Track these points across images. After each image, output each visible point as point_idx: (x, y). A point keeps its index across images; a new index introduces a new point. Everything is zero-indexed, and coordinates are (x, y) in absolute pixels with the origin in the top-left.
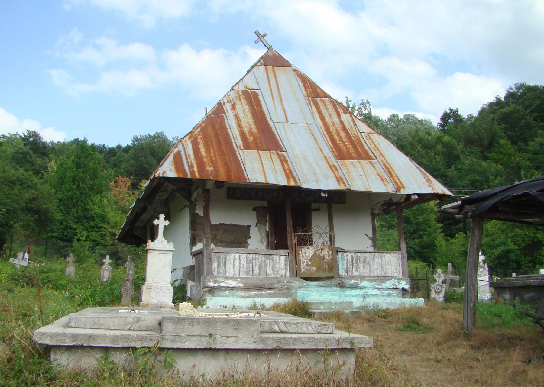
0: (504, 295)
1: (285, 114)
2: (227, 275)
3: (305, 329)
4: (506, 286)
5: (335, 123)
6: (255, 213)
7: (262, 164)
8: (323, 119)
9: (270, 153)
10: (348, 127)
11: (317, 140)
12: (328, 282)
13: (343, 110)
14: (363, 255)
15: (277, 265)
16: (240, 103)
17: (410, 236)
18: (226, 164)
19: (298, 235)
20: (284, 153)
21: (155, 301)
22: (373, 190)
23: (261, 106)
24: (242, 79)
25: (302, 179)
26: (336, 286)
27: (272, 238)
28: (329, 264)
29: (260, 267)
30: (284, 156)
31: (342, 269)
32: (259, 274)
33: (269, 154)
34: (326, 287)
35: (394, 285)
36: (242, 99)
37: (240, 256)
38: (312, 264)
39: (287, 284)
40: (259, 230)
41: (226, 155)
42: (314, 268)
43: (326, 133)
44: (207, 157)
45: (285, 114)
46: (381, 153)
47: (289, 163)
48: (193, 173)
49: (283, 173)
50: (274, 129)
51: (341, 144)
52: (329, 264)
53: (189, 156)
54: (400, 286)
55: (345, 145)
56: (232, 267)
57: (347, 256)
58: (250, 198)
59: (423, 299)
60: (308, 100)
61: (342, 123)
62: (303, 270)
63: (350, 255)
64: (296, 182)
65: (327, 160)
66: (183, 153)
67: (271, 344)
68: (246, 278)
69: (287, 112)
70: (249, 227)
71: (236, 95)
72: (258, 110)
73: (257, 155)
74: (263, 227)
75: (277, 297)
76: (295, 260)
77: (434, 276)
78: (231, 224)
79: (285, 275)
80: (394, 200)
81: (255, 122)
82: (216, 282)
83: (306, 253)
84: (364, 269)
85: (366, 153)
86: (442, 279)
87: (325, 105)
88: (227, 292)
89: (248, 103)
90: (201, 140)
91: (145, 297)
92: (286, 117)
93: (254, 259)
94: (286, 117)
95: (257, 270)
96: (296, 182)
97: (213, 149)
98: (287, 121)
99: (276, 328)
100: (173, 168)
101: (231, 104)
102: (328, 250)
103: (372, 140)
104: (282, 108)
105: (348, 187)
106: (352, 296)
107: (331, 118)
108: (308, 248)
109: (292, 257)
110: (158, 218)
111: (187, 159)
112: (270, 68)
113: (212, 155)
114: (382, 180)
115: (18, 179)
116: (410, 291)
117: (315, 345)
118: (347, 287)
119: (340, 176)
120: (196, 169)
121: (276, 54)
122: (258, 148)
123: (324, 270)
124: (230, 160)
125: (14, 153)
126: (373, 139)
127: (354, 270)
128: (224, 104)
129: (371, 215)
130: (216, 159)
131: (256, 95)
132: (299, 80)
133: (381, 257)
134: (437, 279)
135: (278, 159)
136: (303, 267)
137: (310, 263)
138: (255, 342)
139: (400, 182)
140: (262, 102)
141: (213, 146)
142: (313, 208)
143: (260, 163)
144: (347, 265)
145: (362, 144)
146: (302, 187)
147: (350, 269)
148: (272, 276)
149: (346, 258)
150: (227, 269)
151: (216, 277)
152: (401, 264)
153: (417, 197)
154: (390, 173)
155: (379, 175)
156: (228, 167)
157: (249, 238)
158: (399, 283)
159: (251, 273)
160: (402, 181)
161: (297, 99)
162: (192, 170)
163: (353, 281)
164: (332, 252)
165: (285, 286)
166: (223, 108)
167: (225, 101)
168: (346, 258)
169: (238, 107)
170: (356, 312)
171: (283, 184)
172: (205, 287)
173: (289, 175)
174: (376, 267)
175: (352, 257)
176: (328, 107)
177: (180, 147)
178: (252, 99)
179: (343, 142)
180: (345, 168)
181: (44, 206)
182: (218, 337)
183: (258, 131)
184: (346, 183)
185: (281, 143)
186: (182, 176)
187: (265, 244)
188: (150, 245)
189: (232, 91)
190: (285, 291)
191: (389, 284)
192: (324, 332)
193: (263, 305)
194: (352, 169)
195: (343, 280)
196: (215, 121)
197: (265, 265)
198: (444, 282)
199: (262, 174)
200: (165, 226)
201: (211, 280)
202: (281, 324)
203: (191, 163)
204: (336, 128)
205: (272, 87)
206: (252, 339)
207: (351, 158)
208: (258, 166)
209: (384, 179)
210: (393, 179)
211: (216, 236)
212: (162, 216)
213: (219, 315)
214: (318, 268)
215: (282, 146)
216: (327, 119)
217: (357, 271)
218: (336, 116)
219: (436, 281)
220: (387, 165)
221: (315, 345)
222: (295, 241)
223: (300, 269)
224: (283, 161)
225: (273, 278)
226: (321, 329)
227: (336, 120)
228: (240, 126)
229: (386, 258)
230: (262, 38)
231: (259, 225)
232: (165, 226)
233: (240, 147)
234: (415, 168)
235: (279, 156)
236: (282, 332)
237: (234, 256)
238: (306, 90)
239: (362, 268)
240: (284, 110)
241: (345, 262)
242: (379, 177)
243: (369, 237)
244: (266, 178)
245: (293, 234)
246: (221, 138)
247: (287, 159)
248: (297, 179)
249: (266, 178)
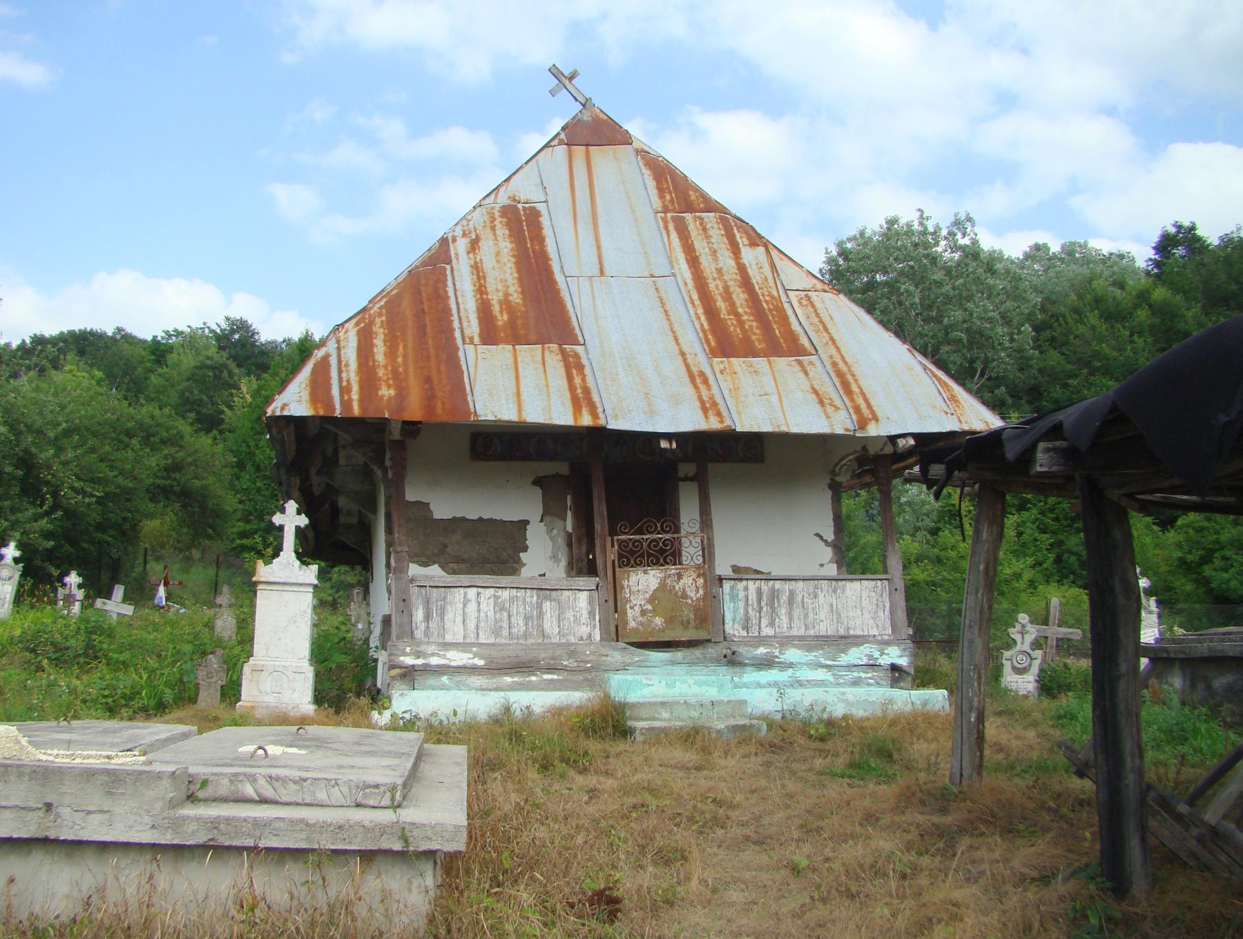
0: (1170, 680)
1: (600, 257)
2: (449, 638)
3: (322, 796)
4: (1173, 655)
5: (725, 269)
6: (537, 493)
7: (517, 378)
8: (693, 262)
9: (543, 349)
10: (756, 279)
11: (670, 313)
12: (698, 652)
13: (749, 238)
14: (787, 586)
15: (569, 615)
16: (491, 235)
17: (1070, 526)
18: (428, 380)
19: (620, 542)
20: (579, 349)
21: (271, 700)
22: (794, 430)
23: (541, 240)
24: (508, 180)
25: (613, 409)
26: (717, 661)
27: (579, 548)
28: (696, 609)
29: (527, 618)
30: (577, 356)
31: (734, 620)
32: (525, 636)
33: (540, 351)
34: (692, 663)
35: (870, 657)
36: (498, 226)
37: (479, 594)
38: (654, 610)
39: (591, 657)
40: (549, 531)
41: (433, 359)
42: (658, 621)
43: (695, 296)
44: (385, 367)
45: (600, 257)
46: (832, 339)
47: (587, 371)
48: (346, 404)
49: (568, 395)
50: (565, 294)
51: (731, 321)
52: (696, 609)
53: (347, 365)
54: (885, 661)
55: (741, 323)
56: (459, 619)
57: (746, 589)
58: (526, 457)
59: (945, 692)
60: (665, 220)
61: (742, 269)
62: (632, 624)
64: (595, 415)
65: (685, 360)
66: (333, 361)
67: (193, 833)
68: (493, 645)
69: (604, 251)
71: (486, 217)
72: (534, 251)
73: (510, 356)
74: (559, 523)
75: (566, 689)
76: (614, 601)
77: (1011, 630)
78: (480, 519)
80: (872, 451)
81: (520, 279)
82: (418, 655)
83: (643, 582)
84: (791, 619)
85: (792, 338)
86: (1029, 638)
87: (705, 229)
88: (445, 679)
89: (510, 236)
90: (382, 326)
91: (249, 692)
92: (601, 263)
93: (512, 599)
94: (601, 263)
95: (519, 625)
96: (595, 415)
97: (405, 347)
98: (602, 273)
99: (249, 790)
100: (306, 395)
101: (468, 240)
102: (694, 576)
103: (813, 306)
104: (594, 243)
105: (728, 422)
106: (759, 685)
107: (716, 260)
108: (645, 572)
109: (607, 593)
110: (283, 511)
111: (340, 372)
112: (579, 151)
113: (400, 360)
114: (821, 403)
115: (141, 426)
116: (912, 671)
117: (308, 839)
118: (746, 665)
119: (712, 398)
120: (355, 396)
121: (602, 115)
122: (516, 337)
123: (685, 625)
124: (439, 370)
125: (196, 367)
126: (818, 305)
127: (764, 622)
128: (454, 240)
129: (831, 487)
130: (406, 370)
131: (533, 215)
132: (647, 173)
133: (835, 591)
134: (1018, 637)
135: (562, 364)
136: (633, 617)
137: (650, 607)
138: (153, 827)
139: (869, 406)
140: (547, 231)
141: (405, 341)
142: (681, 475)
143: (514, 376)
144: (747, 612)
145: (786, 318)
146: (609, 427)
148: (556, 640)
149: (742, 594)
150: (448, 625)
151: (419, 643)
152: (888, 605)
153: (912, 442)
154: (846, 386)
155: (816, 392)
156: (431, 388)
157: (525, 549)
158: (882, 654)
159: (505, 633)
160: (873, 403)
161: (636, 220)
162: (346, 400)
163: (762, 650)
164: (705, 581)
165: (588, 662)
166: (448, 250)
167: (459, 232)
168: (742, 594)
169: (486, 246)
170: (744, 726)
171: (563, 423)
172: (392, 667)
173: (581, 398)
174: (822, 615)
175: (759, 593)
176: (711, 232)
177: (331, 347)
178: (523, 225)
179: (737, 315)
180: (729, 377)
181: (197, 483)
182: (65, 812)
183: (524, 299)
184: (725, 413)
185: (575, 324)
186: (321, 413)
187: (564, 563)
188: (264, 571)
189: (478, 209)
190: (589, 674)
191: (856, 655)
192: (372, 803)
193: (528, 708)
194: (745, 380)
195: (735, 648)
196: (423, 282)
197: (541, 615)
198: (1036, 645)
199: (513, 399)
200: (298, 528)
201: (408, 649)
202: (262, 782)
203: (348, 381)
204: (726, 282)
205: (578, 193)
206: (148, 820)
207: (750, 351)
208: (505, 382)
209: (827, 402)
210: (852, 400)
211: (445, 546)
212: (292, 506)
213: (89, 757)
214: (670, 620)
215: (577, 331)
216: (706, 262)
217: (772, 624)
218: (728, 254)
219: (1015, 641)
220: (842, 366)
221: (308, 839)
222: (612, 555)
224: (573, 366)
225: (559, 645)
226: (365, 796)
227: (727, 262)
228: (481, 290)
229: (848, 593)
230: (566, 82)
231: (548, 518)
232: (298, 528)
233: (472, 339)
234: (919, 369)
235: (564, 354)
236: (264, 801)
237: (465, 594)
238: (661, 197)
239: (784, 620)
240: (599, 247)
241: (741, 604)
242: (814, 396)
243: (826, 541)
244: (520, 411)
245: (609, 539)
246: (427, 319)
247: (584, 361)
248: (600, 410)
249: (520, 411)
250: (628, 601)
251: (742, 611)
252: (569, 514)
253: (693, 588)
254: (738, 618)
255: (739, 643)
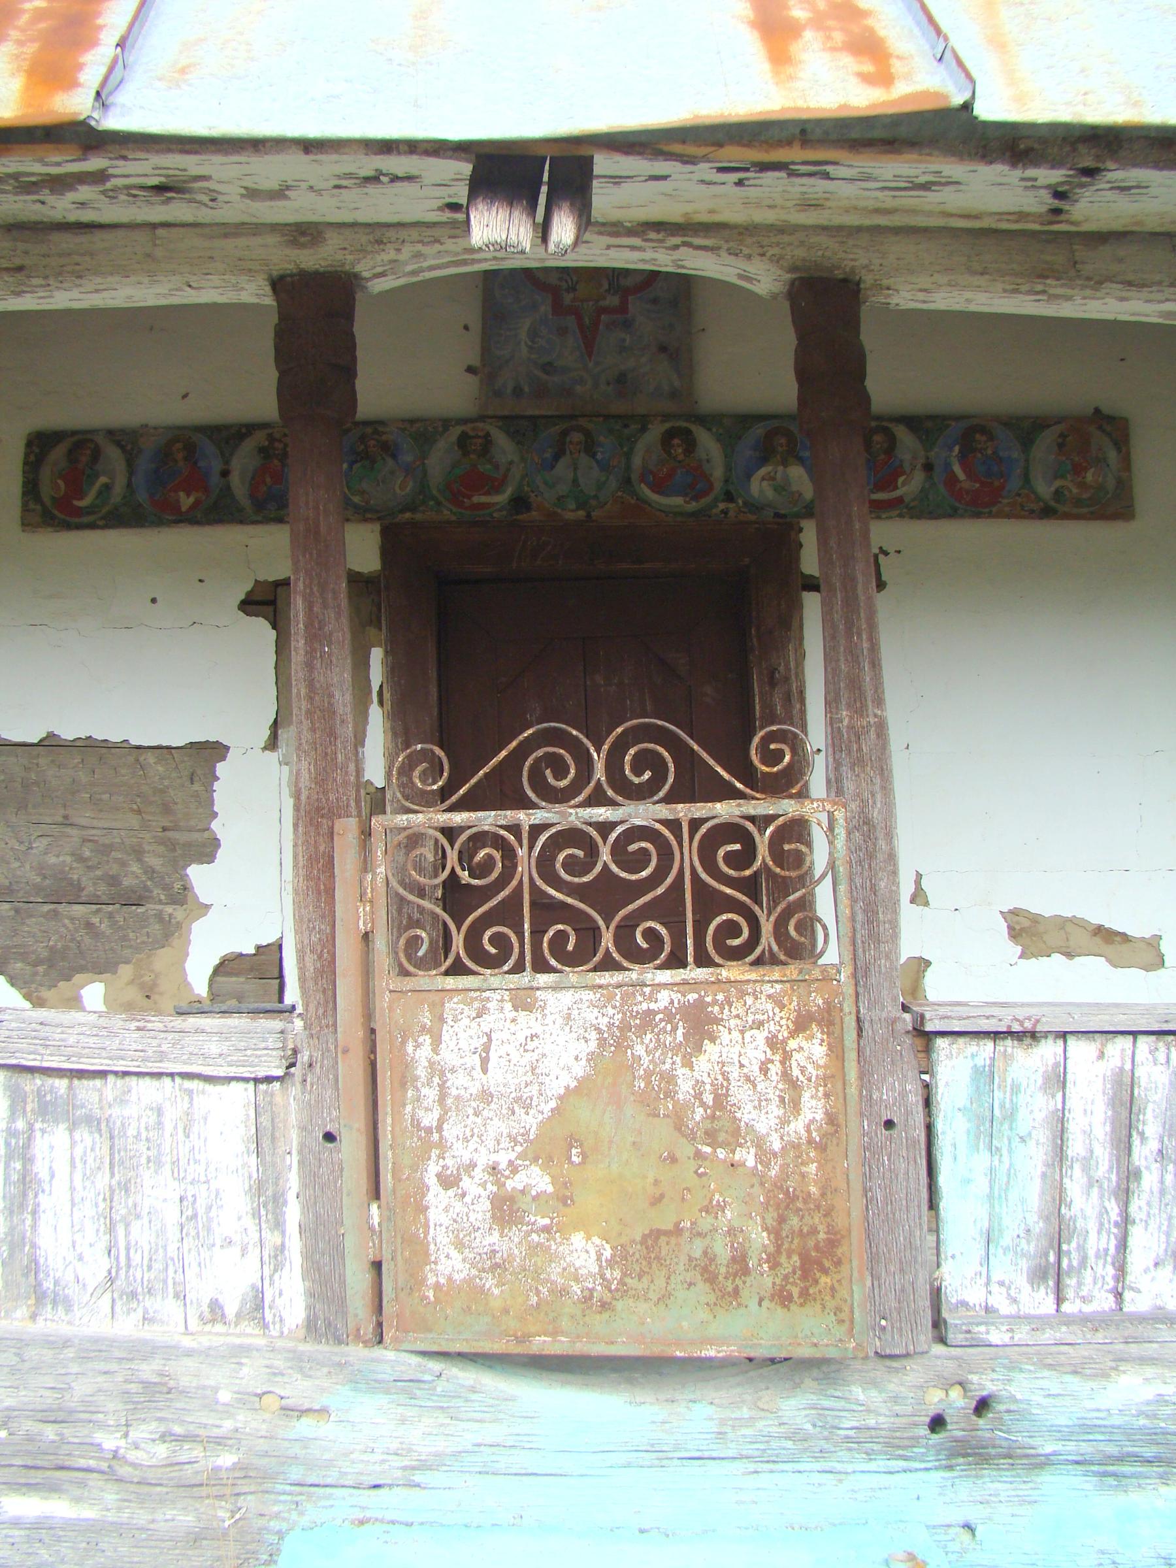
12: (795, 1407)
15: (158, 1193)
42: (583, 1255)
57: (1058, 1080)
58: (218, 511)
62: (449, 1265)
63: (1090, 1068)
70: (209, 753)
76: (364, 1141)
78: (50, 743)
79: (256, 1306)
108: (523, 1002)
118: (1042, 1463)
136: (454, 1233)
137: (537, 1179)
147: (1097, 1241)
148: (94, 1320)
149: (1035, 1108)
157: (207, 850)
164: (836, 1050)
195: (985, 1384)
214: (645, 1253)
223: (419, 1252)
225: (95, 1350)
250: (430, 1141)
251: (1029, 1194)
252: (376, 717)
253: (771, 1086)
254: (1011, 1228)
255: (1013, 1358)
